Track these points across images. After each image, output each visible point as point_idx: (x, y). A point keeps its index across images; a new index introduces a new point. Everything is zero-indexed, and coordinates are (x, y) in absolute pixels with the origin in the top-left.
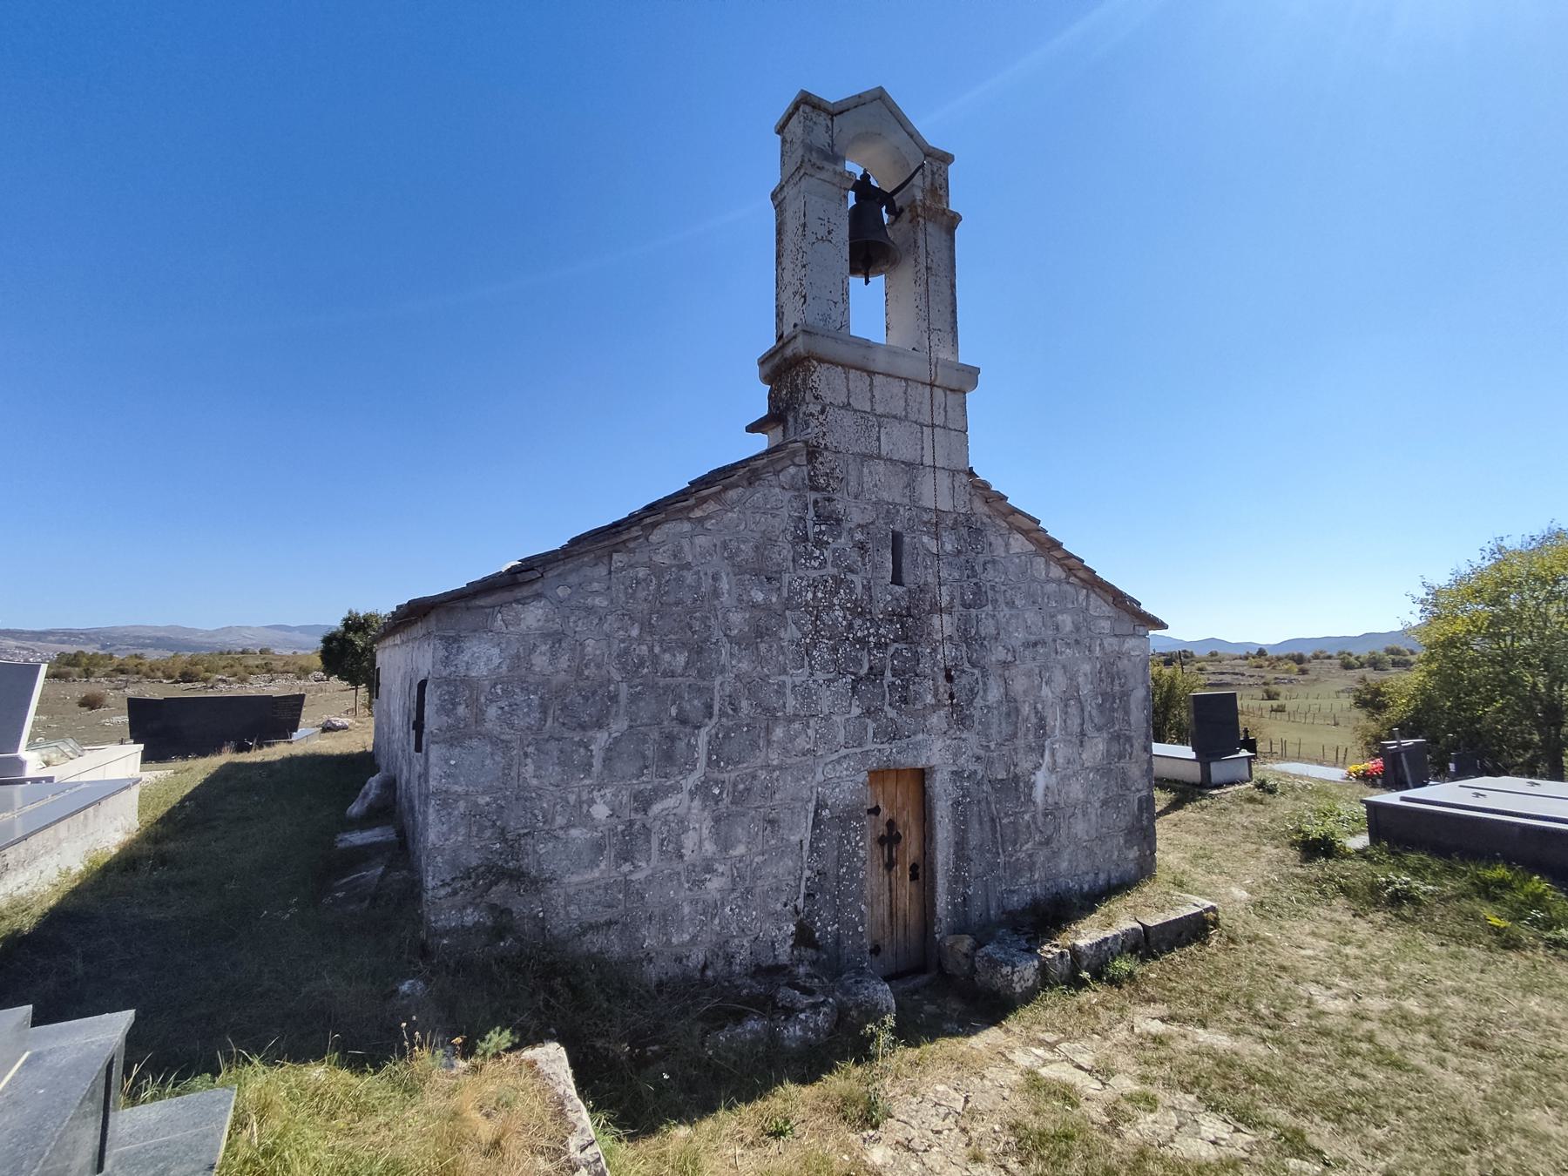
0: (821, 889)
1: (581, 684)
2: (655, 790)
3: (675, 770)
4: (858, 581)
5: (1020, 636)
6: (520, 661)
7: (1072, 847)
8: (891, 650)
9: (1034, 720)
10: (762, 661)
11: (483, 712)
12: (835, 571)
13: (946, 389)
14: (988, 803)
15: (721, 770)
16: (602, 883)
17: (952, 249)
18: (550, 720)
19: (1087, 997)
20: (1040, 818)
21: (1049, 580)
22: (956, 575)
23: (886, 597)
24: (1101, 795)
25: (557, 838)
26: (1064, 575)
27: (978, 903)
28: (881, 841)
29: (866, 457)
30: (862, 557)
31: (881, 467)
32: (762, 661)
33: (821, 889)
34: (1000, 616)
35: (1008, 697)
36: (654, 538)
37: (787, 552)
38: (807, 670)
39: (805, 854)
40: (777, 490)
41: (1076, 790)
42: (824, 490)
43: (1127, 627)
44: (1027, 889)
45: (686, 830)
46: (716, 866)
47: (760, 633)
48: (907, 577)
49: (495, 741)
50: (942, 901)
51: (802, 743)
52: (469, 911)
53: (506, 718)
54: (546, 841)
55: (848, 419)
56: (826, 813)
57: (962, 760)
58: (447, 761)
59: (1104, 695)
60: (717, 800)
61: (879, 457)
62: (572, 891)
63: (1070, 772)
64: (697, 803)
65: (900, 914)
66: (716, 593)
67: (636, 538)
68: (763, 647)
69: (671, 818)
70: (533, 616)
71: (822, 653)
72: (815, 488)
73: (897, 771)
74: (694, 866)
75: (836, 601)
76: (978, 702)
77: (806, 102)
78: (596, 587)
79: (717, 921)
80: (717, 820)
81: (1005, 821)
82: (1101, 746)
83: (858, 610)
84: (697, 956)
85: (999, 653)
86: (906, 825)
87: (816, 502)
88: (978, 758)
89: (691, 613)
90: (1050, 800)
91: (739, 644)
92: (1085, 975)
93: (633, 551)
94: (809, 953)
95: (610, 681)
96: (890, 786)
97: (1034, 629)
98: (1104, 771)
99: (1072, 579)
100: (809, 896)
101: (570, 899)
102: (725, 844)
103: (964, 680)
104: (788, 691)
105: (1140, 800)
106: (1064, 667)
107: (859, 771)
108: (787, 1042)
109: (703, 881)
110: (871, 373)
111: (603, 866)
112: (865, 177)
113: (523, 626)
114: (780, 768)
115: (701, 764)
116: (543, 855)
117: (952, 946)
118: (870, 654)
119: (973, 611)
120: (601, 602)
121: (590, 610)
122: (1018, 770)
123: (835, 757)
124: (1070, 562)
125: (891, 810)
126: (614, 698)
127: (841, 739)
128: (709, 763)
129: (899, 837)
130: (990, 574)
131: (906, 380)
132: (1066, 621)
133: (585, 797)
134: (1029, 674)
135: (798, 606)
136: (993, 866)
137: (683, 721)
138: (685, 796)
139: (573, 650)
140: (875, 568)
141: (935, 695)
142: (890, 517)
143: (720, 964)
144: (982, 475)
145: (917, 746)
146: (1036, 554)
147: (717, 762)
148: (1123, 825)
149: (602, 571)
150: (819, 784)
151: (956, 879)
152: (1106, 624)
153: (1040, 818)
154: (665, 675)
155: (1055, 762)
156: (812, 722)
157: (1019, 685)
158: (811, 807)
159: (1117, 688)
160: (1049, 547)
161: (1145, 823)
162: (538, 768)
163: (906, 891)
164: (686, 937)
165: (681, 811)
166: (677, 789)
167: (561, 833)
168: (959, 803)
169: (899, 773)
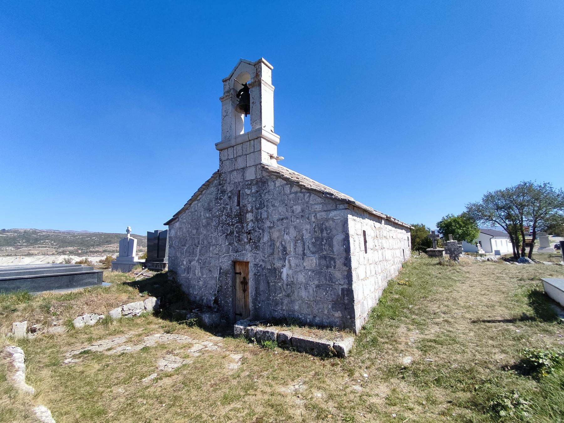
5: (276, 217)
6: (176, 233)
8: (236, 226)
9: (281, 248)
10: (208, 231)
20: (285, 286)
21: (291, 193)
22: (254, 200)
24: (316, 282)
26: (299, 190)
35: (271, 240)
41: (301, 278)
47: (208, 224)
57: (257, 260)
59: (317, 239)
60: (200, 263)
63: (298, 270)
66: (201, 216)
71: (220, 228)
72: (220, 185)
73: (240, 262)
77: (224, 81)
81: (271, 284)
83: (228, 215)
90: (289, 280)
97: (282, 213)
98: (318, 272)
100: (218, 292)
102: (202, 275)
103: (256, 234)
105: (343, 289)
106: (295, 227)
110: (233, 147)
114: (211, 257)
115: (198, 255)
120: (185, 221)
121: (184, 222)
126: (187, 240)
127: (224, 251)
128: (200, 255)
134: (279, 231)
136: (268, 299)
143: (201, 301)
145: (243, 255)
152: (318, 207)
153: (285, 286)
155: (290, 265)
157: (275, 235)
158: (219, 268)
159: (325, 234)
161: (346, 302)
166: (194, 260)
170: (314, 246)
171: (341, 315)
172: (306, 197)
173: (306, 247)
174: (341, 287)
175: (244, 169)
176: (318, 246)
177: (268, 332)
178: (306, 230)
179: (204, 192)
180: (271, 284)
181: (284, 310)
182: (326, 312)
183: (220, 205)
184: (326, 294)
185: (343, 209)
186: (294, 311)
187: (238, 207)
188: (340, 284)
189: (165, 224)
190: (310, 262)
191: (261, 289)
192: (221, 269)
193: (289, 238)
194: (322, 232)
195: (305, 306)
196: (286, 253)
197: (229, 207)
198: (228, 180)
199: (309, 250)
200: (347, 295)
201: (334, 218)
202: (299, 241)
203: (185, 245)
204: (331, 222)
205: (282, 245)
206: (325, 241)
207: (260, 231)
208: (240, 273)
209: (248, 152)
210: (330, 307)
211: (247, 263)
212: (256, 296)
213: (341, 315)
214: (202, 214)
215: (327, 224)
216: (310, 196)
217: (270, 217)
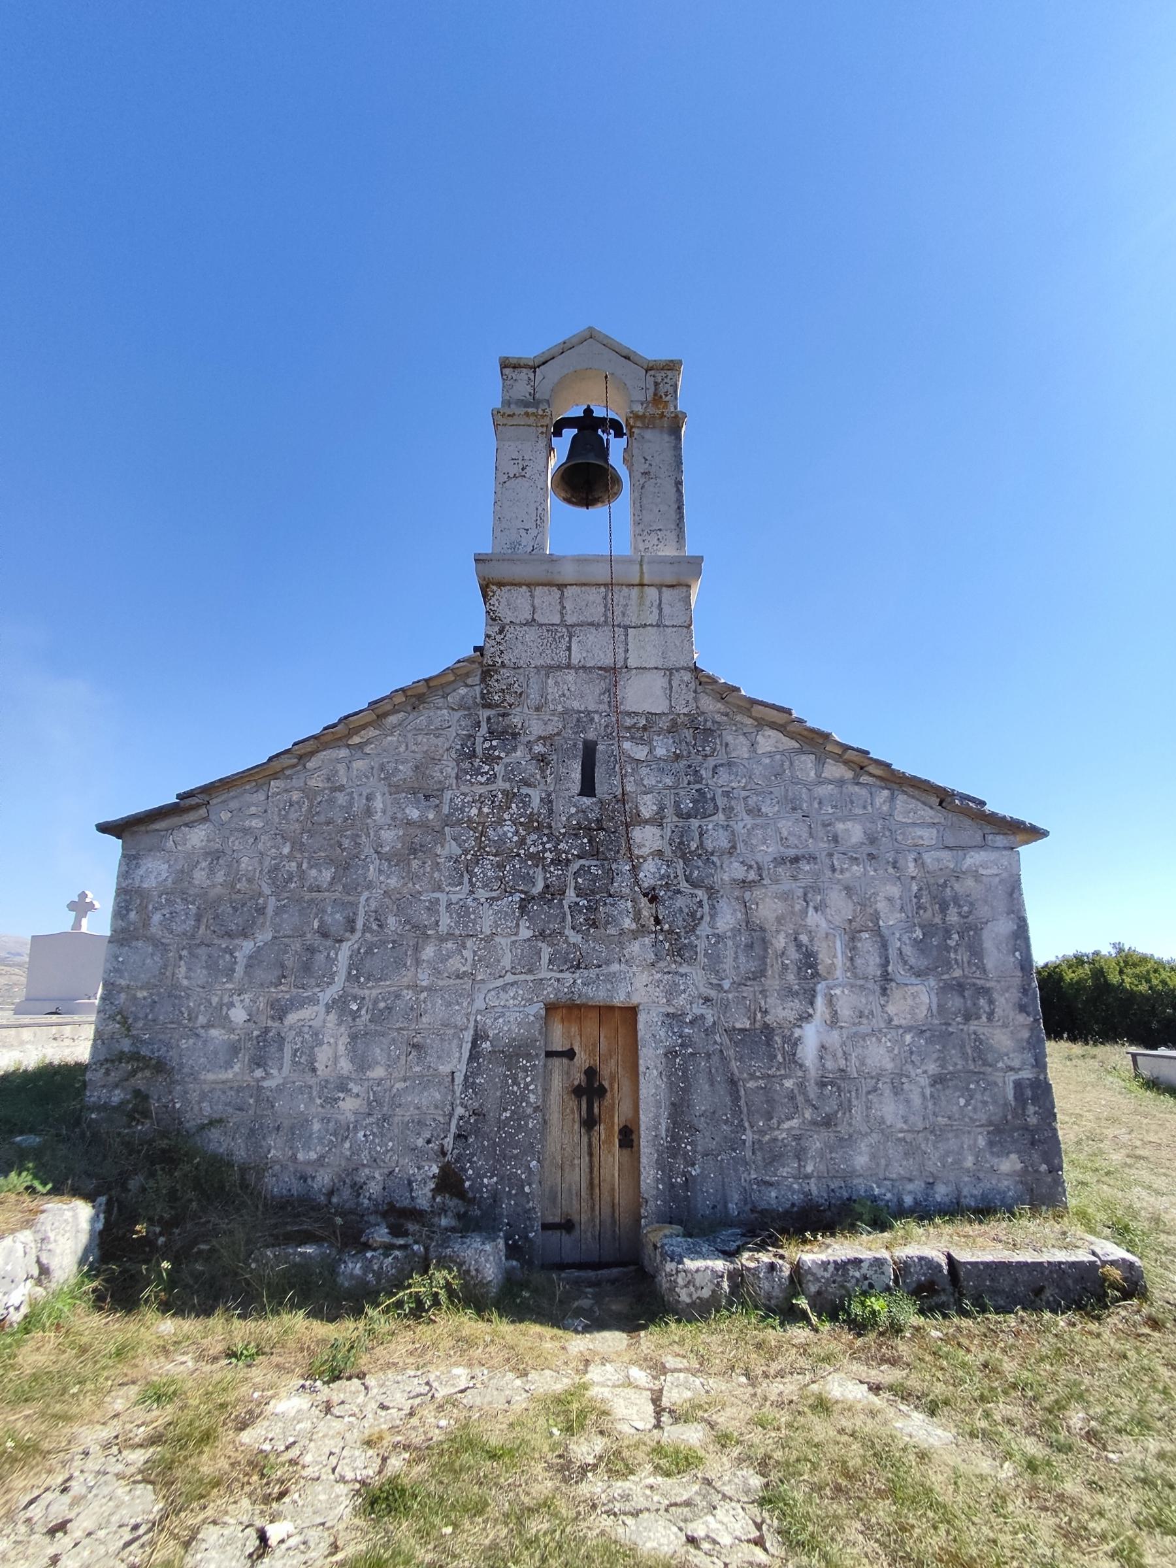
0: (477, 1132)
1: (234, 896)
2: (291, 1000)
3: (313, 982)
4: (536, 795)
5: (767, 851)
6: (183, 875)
7: (875, 1137)
8: (575, 866)
9: (794, 954)
11: (150, 918)
12: (507, 786)
13: (660, 586)
14: (723, 1058)
15: (362, 986)
16: (236, 1085)
17: (677, 448)
18: (203, 928)
19: (799, 1333)
20: (812, 1090)
21: (820, 781)
22: (669, 781)
23: (570, 806)
24: (932, 1068)
25: (197, 1035)
26: (849, 775)
27: (709, 1188)
28: (578, 1092)
29: (550, 669)
30: (543, 771)
31: (571, 676)
32: (414, 877)
33: (477, 1132)
34: (738, 827)
36: (310, 765)
37: (451, 770)
38: (466, 887)
39: (458, 1089)
40: (445, 712)
41: (879, 1055)
42: (497, 706)
43: (970, 833)
44: (789, 1184)
45: (321, 1044)
46: (351, 1085)
48: (601, 789)
49: (158, 944)
50: (649, 1176)
51: (455, 964)
52: (117, 1092)
53: (166, 925)
54: (188, 1037)
55: (531, 634)
56: (486, 1045)
57: (681, 1000)
58: (116, 957)
59: (929, 930)
61: (569, 666)
62: (206, 1088)
63: (864, 1029)
64: (333, 1017)
65: (605, 1187)
66: (369, 812)
67: (294, 766)
68: (415, 864)
69: (306, 1029)
70: (197, 837)
71: (486, 868)
74: (327, 1081)
75: (506, 816)
76: (704, 929)
77: (505, 364)
78: (253, 810)
79: (347, 1145)
80: (354, 1037)
82: (925, 999)
84: (323, 1179)
85: (736, 870)
86: (612, 1078)
87: (489, 719)
88: (707, 1000)
89: (341, 832)
90: (830, 1065)
91: (388, 860)
92: (803, 1303)
93: (290, 777)
94: (453, 1203)
95: (260, 895)
96: (591, 1026)
97: (793, 840)
98: (936, 1034)
99: (864, 779)
101: (203, 1096)
102: (362, 1064)
103: (680, 902)
104: (442, 909)
105: (1018, 1085)
106: (848, 889)
107: (531, 1002)
108: (340, 1280)
109: (336, 1100)
110: (561, 587)
111: (237, 1068)
112: (588, 411)
113: (189, 846)
114: (428, 989)
115: (340, 979)
116: (185, 1050)
118: (545, 870)
119: (695, 823)
120: (256, 823)
121: (246, 831)
122: (769, 1019)
123: (500, 982)
124: (850, 755)
125: (592, 1053)
126: (261, 910)
127: (506, 962)
130: (724, 776)
131: (605, 585)
132: (854, 832)
133: (226, 999)
134: (786, 896)
135: (459, 822)
136: (735, 1144)
137: (325, 935)
138: (321, 1008)
139: (229, 866)
140: (558, 779)
141: (637, 917)
142: (580, 726)
143: (347, 1193)
144: (709, 667)
145: (611, 978)
146: (801, 751)
147: (357, 977)
148: (982, 1117)
149: (261, 796)
150: (478, 1012)
151: (672, 1149)
152: (928, 836)
153: (812, 1090)
154: (311, 890)
156: (469, 943)
157: (768, 909)
158: (468, 1036)
159: (953, 917)
160: (815, 742)
161: (1033, 1120)
162: (189, 969)
163: (612, 1159)
164: (313, 1156)
165: (316, 1024)
167: (202, 1031)
168: (676, 1054)
169: (605, 1011)
170: (922, 951)
171: (1019, 1166)
172: (878, 801)
173: (893, 954)
174: (1012, 1077)
175: (613, 673)
176: (935, 953)
177: (857, 1262)
178: (890, 899)
179: (393, 719)
180: (751, 1084)
181: (807, 1177)
182: (969, 1162)
183: (492, 779)
184: (967, 1104)
185: (1005, 848)
186: (852, 1173)
187: (587, 801)
188: (1011, 1069)
189: (104, 828)
190: (910, 1001)
191: (699, 1108)
193: (823, 924)
194: (944, 909)
195: (894, 1151)
196: (816, 974)
197: (536, 795)
198: (534, 697)
199: (905, 963)
200: (1035, 1100)
201: (981, 871)
202: (865, 935)
203: (245, 934)
204: (970, 882)
205: (799, 946)
206: (956, 936)
207: (701, 894)
208: (570, 1054)
209: (634, 620)
210: (982, 1142)
211: (632, 1012)
212: (675, 1137)
213: (1019, 1166)
214: (378, 804)
215: (957, 886)
216: (892, 798)
217: (740, 846)
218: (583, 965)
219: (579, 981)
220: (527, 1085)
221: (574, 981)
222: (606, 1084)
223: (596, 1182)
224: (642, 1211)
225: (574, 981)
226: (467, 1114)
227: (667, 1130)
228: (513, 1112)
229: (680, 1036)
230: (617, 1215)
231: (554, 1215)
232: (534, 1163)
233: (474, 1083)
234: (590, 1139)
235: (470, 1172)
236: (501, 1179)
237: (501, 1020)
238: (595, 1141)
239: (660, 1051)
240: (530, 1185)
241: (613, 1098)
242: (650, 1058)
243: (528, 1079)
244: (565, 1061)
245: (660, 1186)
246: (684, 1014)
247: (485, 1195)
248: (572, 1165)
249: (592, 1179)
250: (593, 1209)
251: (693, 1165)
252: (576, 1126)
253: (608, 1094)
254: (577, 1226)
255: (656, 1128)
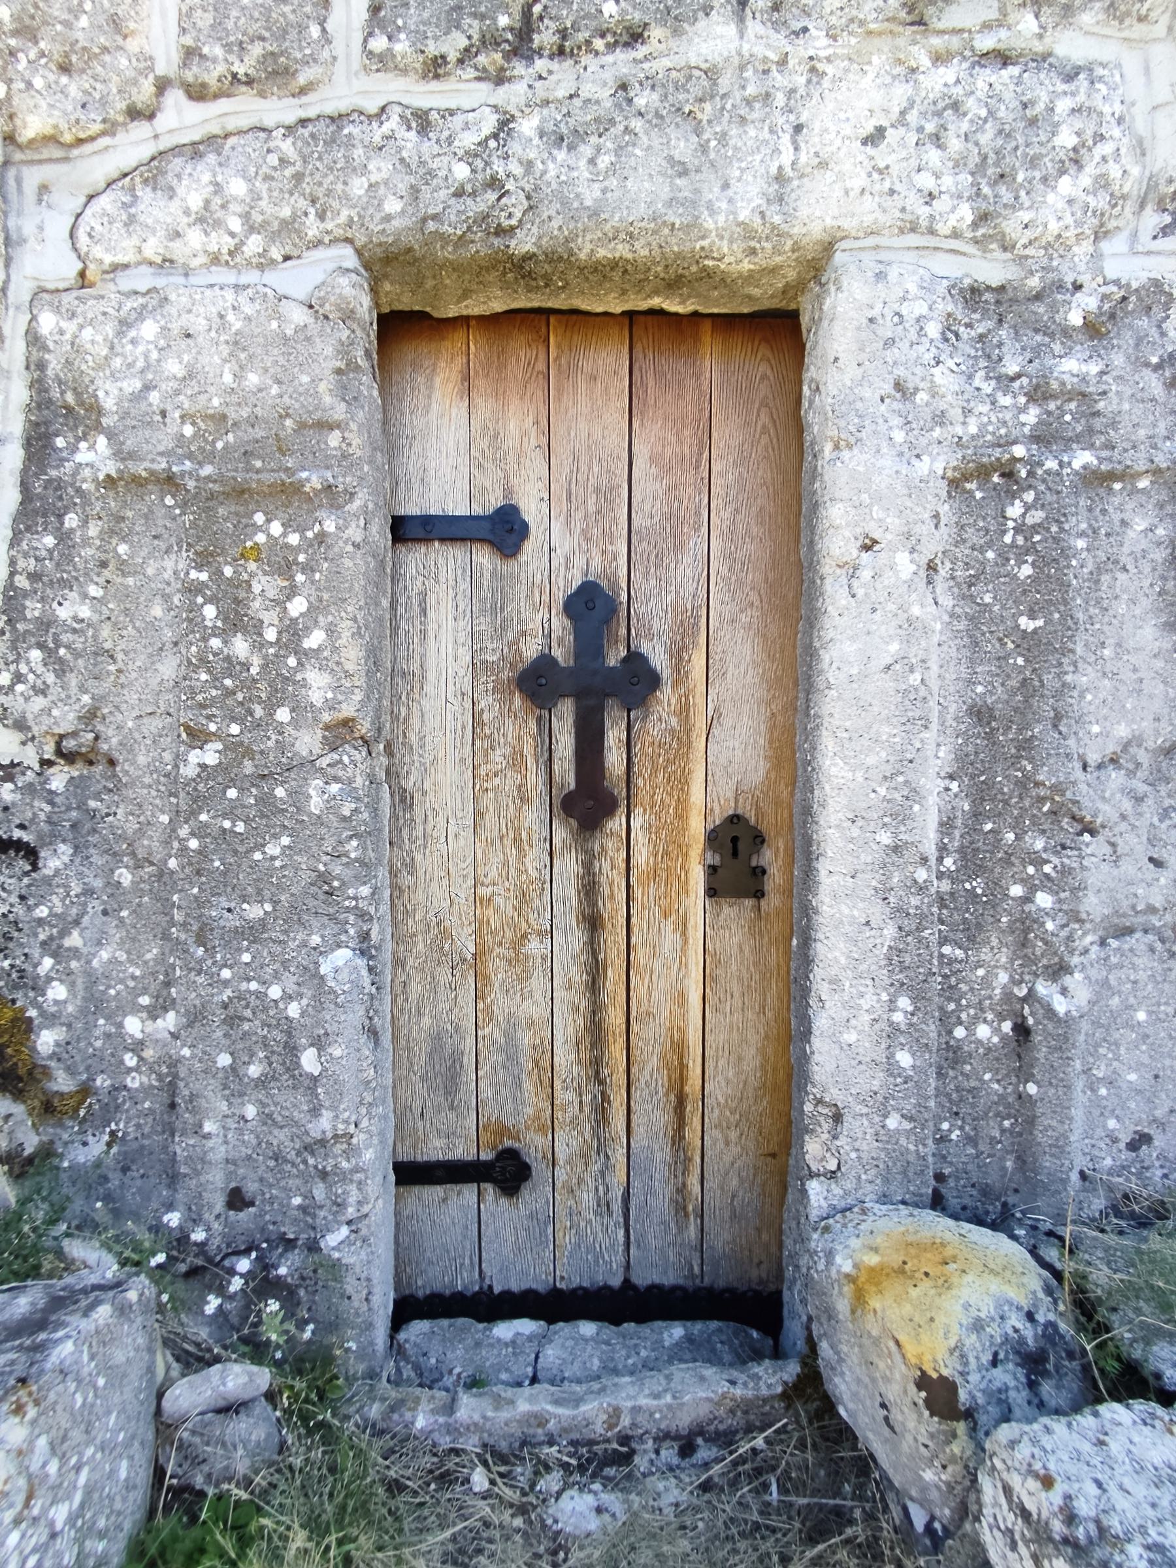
28: (537, 683)
33: (82, 830)
56: (93, 457)
57: (1055, 208)
65: (651, 1039)
86: (684, 631)
117: (863, 1285)
123: (133, 146)
129: (638, 682)
145: (694, 99)
163: (682, 947)
191: (1099, 733)
192: (54, 418)
208: (503, 531)
218: (545, 37)
219: (527, 126)
220: (292, 633)
221: (505, 124)
222: (657, 655)
223: (614, 1017)
224: (813, 1148)
225: (505, 124)
226: (30, 756)
227: (946, 826)
228: (236, 750)
229: (1038, 394)
230: (692, 1133)
231: (450, 1135)
232: (343, 955)
233: (46, 623)
234: (588, 866)
235: (57, 992)
236: (195, 1018)
237: (149, 329)
238: (610, 872)
239: (937, 463)
240: (319, 1044)
241: (684, 712)
242: (881, 489)
243: (297, 606)
244: (483, 558)
245: (904, 1059)
246: (1058, 289)
247: (134, 1082)
248: (520, 960)
249: (596, 1010)
250: (601, 1113)
251: (1058, 971)
252: (535, 818)
253: (666, 696)
254: (539, 1170)
255: (899, 816)
